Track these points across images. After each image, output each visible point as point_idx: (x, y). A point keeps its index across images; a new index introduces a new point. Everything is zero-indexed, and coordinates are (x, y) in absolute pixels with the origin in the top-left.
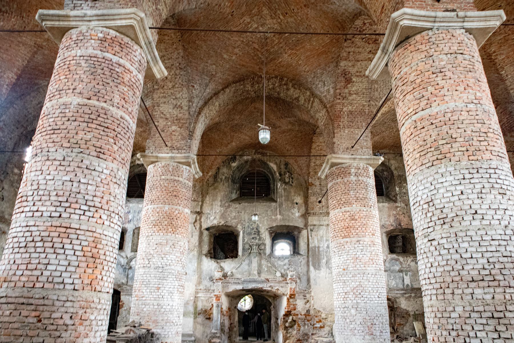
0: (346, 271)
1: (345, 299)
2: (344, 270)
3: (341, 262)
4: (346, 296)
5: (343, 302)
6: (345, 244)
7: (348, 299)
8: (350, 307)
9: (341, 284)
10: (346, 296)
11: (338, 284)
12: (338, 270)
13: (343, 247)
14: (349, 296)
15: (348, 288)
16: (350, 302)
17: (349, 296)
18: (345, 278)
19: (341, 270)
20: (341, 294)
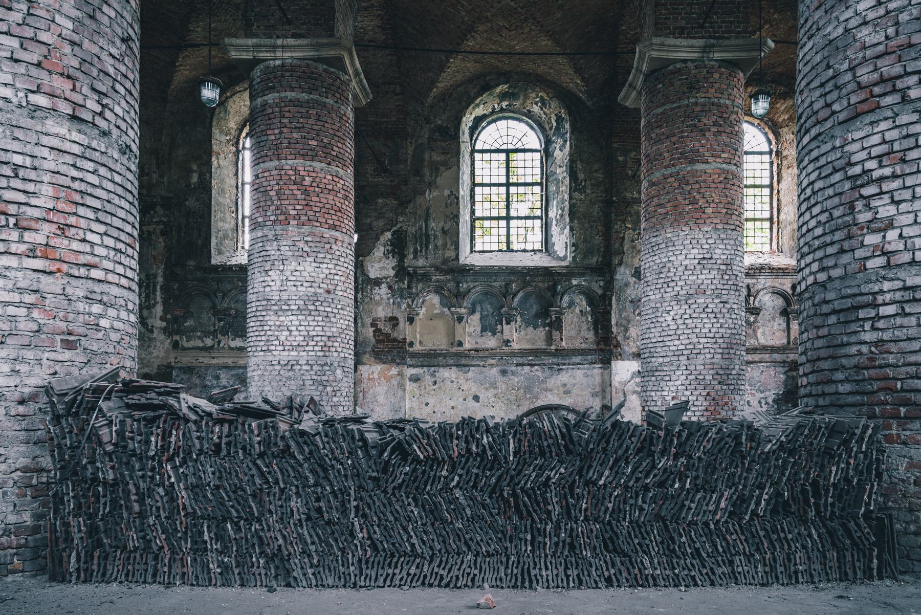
0: (332, 296)
1: (326, 349)
2: (328, 292)
3: (322, 276)
4: (330, 344)
5: (322, 354)
6: (332, 241)
7: (333, 349)
8: (336, 364)
9: (320, 318)
10: (330, 344)
11: (309, 318)
12: (312, 290)
13: (328, 246)
14: (336, 344)
15: (334, 330)
16: (335, 354)
17: (336, 344)
18: (329, 309)
19: (322, 291)
20: (319, 339)
